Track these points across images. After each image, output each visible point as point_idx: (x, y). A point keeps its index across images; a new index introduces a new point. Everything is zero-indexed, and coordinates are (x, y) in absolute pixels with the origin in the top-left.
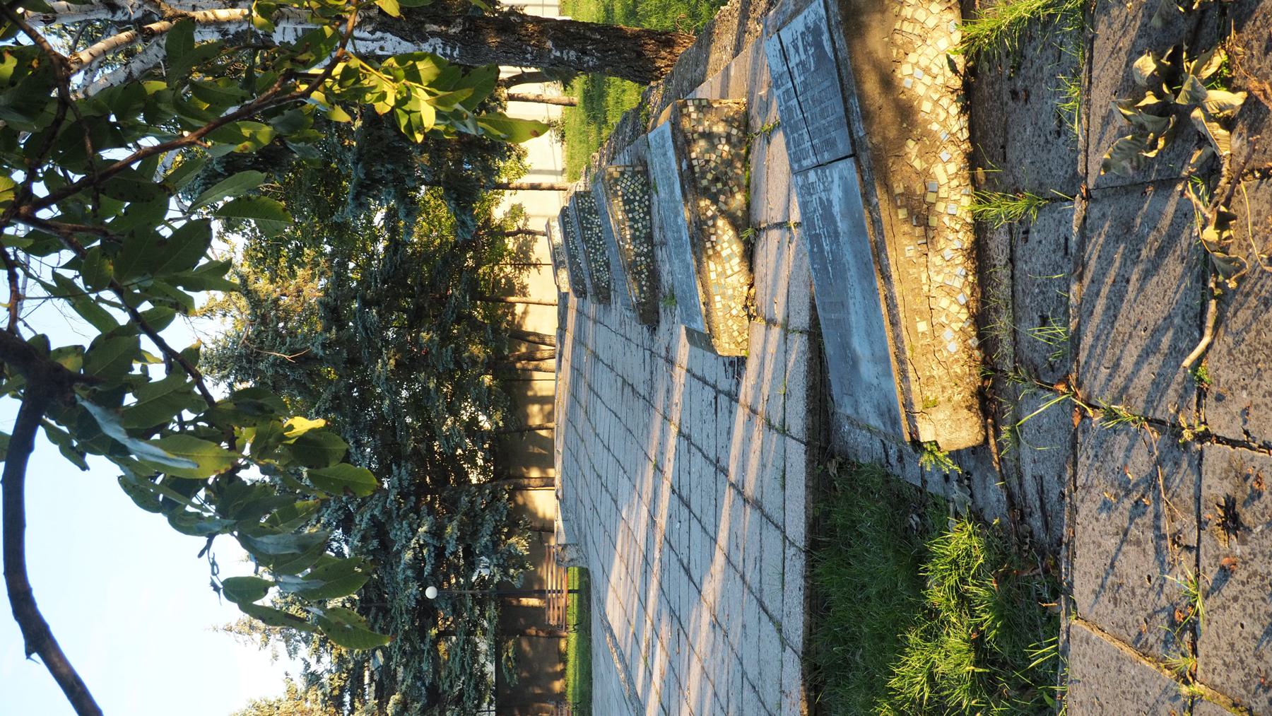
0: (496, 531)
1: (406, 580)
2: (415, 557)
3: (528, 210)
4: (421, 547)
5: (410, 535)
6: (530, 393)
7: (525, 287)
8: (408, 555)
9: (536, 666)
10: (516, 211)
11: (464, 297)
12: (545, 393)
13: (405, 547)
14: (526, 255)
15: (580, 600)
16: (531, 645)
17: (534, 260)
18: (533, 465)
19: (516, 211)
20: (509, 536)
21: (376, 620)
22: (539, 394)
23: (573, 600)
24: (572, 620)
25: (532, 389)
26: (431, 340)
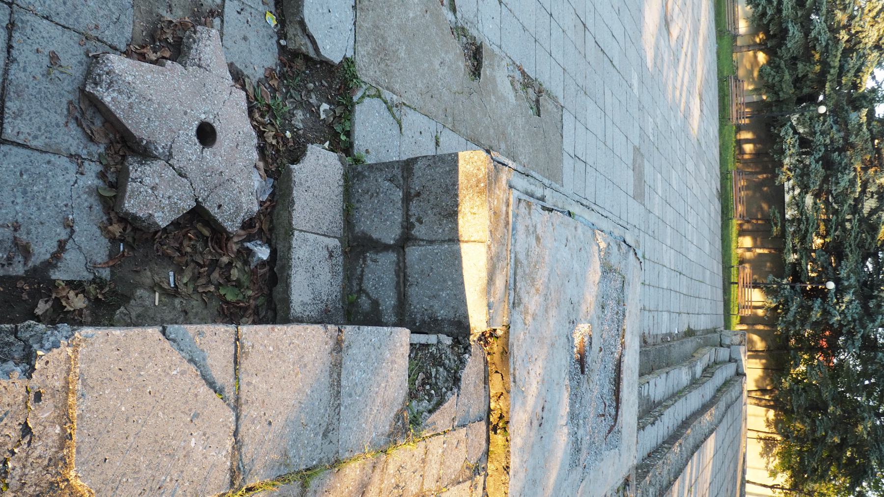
0: (787, 311)
1: (848, 278)
2: (842, 297)
3: (767, 474)
4: (838, 303)
5: (846, 311)
6: (764, 361)
7: (768, 426)
8: (847, 299)
9: (758, 195)
10: (773, 474)
11: (809, 462)
12: (754, 361)
13: (851, 302)
14: (766, 444)
15: (729, 278)
16: (762, 208)
17: (762, 442)
18: (762, 317)
19: (773, 474)
20: (776, 308)
21: (870, 244)
22: (758, 361)
23: (734, 279)
24: (734, 271)
25: (763, 364)
26: (832, 438)
